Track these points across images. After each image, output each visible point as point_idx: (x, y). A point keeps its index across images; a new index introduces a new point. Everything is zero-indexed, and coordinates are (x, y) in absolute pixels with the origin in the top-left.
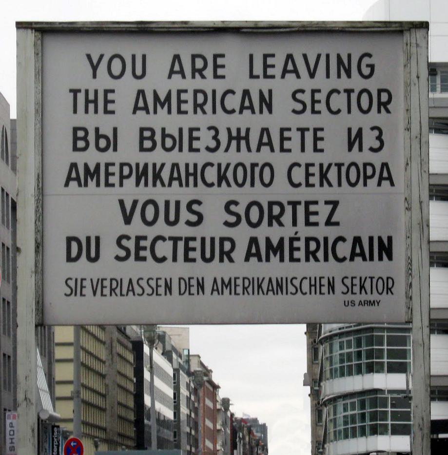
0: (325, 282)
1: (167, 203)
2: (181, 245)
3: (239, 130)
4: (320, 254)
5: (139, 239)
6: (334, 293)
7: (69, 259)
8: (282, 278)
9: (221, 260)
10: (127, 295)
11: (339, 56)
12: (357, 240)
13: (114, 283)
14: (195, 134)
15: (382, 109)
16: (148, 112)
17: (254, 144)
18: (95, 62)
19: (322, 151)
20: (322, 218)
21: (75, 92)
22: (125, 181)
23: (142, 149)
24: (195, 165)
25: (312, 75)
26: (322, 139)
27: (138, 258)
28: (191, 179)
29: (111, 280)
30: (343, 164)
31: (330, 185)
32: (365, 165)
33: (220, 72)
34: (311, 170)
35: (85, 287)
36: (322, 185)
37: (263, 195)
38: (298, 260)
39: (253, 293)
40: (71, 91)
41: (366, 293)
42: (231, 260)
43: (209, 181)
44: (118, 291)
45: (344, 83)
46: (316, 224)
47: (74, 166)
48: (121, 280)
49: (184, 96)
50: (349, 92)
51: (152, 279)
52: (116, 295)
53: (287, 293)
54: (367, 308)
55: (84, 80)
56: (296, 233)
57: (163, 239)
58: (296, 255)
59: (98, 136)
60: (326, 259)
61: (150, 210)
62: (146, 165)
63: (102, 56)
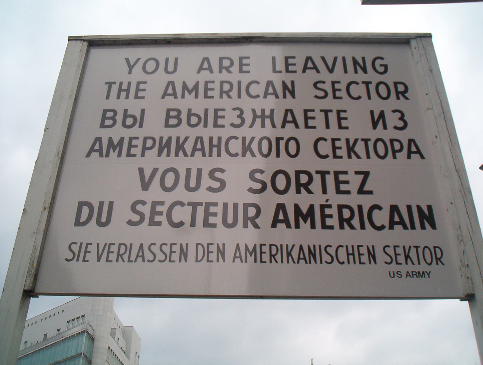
0: (363, 250)
1: (189, 171)
2: (201, 210)
3: (263, 111)
4: (356, 222)
5: (155, 204)
6: (375, 263)
7: (78, 223)
8: (314, 246)
9: (245, 226)
10: (135, 261)
11: (354, 59)
12: (394, 209)
13: (123, 248)
14: (220, 113)
15: (400, 95)
16: (176, 97)
17: (278, 121)
18: (132, 63)
19: (347, 128)
20: (354, 186)
21: (110, 84)
22: (147, 152)
23: (167, 125)
24: (220, 139)
25: (331, 71)
26: (346, 119)
27: (152, 223)
28: (215, 150)
29: (120, 245)
30: (369, 140)
31: (358, 157)
32: (392, 141)
33: (245, 68)
34: (337, 144)
35: (90, 252)
36: (350, 157)
37: (291, 166)
38: (331, 227)
39: (282, 262)
40: (106, 83)
41: (413, 264)
42: (256, 226)
43: (233, 152)
44: (126, 257)
45: (361, 77)
46: (348, 192)
47: (99, 140)
48: (131, 245)
49: (210, 86)
50: (367, 84)
51: (166, 244)
52: (124, 261)
53: (321, 262)
54: (416, 280)
55: (121, 75)
56: (327, 201)
57: (182, 204)
58: (329, 222)
59: (126, 115)
60: (363, 227)
61: (170, 177)
62: (170, 139)
63: (139, 59)
